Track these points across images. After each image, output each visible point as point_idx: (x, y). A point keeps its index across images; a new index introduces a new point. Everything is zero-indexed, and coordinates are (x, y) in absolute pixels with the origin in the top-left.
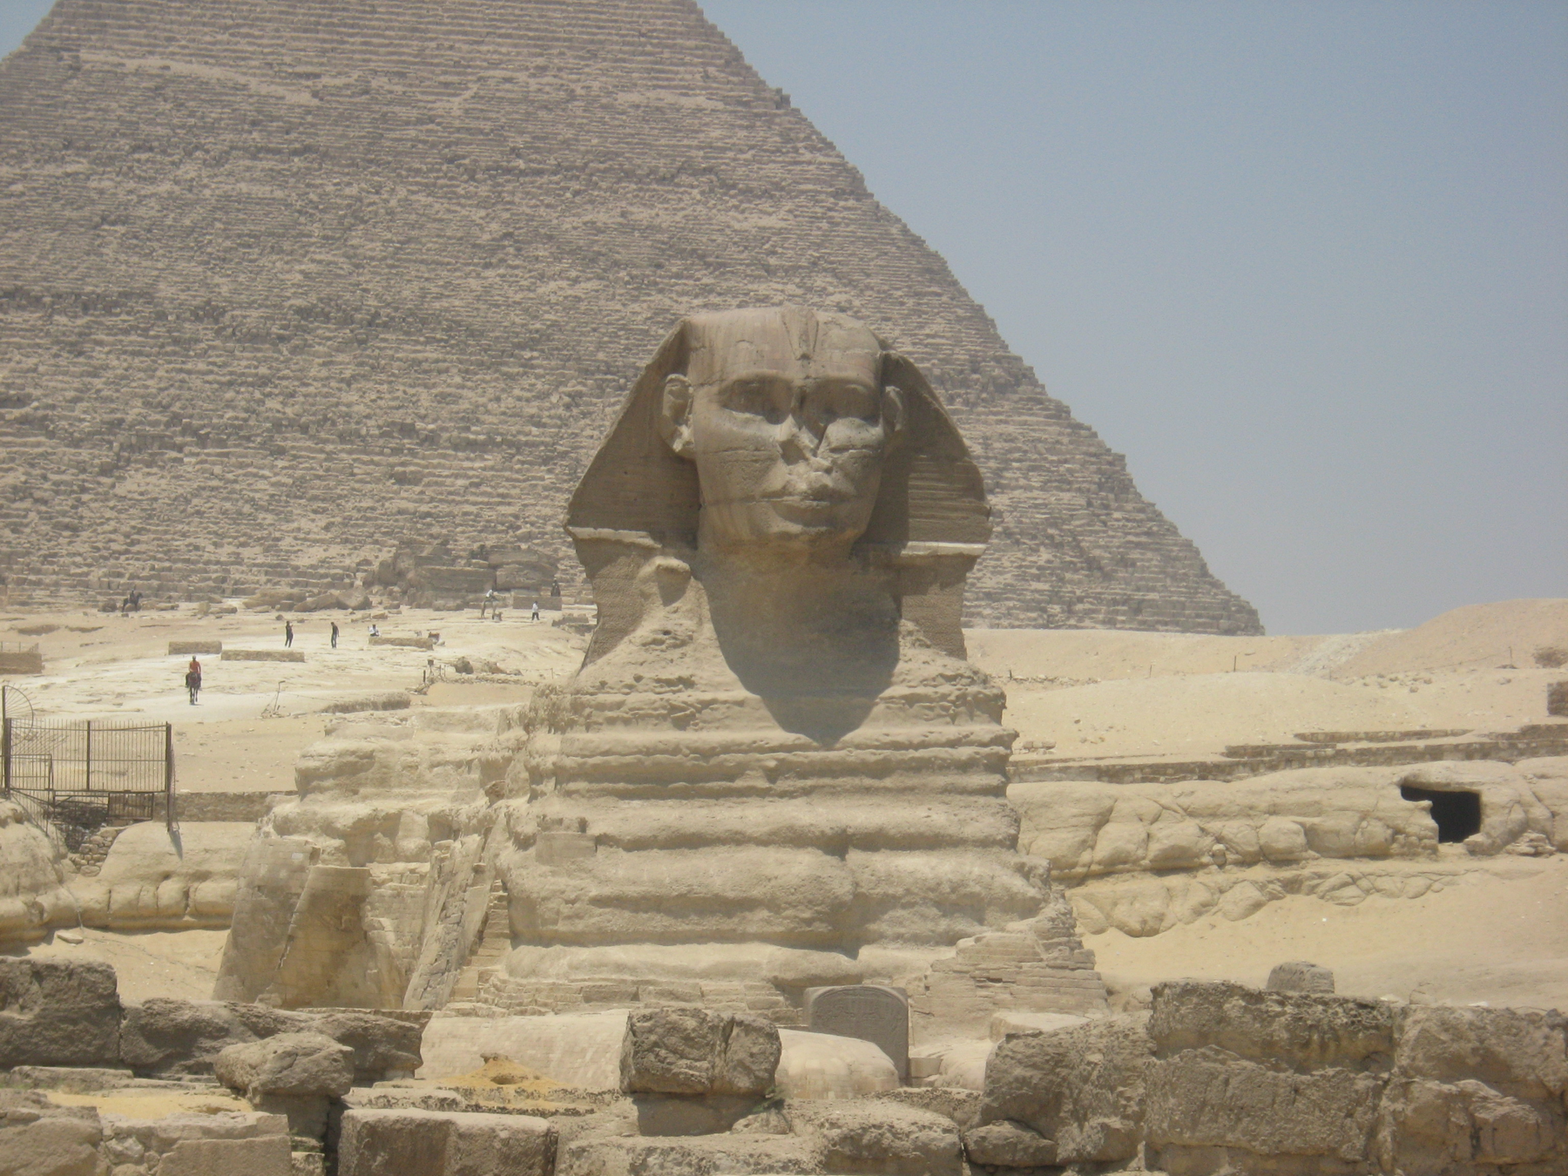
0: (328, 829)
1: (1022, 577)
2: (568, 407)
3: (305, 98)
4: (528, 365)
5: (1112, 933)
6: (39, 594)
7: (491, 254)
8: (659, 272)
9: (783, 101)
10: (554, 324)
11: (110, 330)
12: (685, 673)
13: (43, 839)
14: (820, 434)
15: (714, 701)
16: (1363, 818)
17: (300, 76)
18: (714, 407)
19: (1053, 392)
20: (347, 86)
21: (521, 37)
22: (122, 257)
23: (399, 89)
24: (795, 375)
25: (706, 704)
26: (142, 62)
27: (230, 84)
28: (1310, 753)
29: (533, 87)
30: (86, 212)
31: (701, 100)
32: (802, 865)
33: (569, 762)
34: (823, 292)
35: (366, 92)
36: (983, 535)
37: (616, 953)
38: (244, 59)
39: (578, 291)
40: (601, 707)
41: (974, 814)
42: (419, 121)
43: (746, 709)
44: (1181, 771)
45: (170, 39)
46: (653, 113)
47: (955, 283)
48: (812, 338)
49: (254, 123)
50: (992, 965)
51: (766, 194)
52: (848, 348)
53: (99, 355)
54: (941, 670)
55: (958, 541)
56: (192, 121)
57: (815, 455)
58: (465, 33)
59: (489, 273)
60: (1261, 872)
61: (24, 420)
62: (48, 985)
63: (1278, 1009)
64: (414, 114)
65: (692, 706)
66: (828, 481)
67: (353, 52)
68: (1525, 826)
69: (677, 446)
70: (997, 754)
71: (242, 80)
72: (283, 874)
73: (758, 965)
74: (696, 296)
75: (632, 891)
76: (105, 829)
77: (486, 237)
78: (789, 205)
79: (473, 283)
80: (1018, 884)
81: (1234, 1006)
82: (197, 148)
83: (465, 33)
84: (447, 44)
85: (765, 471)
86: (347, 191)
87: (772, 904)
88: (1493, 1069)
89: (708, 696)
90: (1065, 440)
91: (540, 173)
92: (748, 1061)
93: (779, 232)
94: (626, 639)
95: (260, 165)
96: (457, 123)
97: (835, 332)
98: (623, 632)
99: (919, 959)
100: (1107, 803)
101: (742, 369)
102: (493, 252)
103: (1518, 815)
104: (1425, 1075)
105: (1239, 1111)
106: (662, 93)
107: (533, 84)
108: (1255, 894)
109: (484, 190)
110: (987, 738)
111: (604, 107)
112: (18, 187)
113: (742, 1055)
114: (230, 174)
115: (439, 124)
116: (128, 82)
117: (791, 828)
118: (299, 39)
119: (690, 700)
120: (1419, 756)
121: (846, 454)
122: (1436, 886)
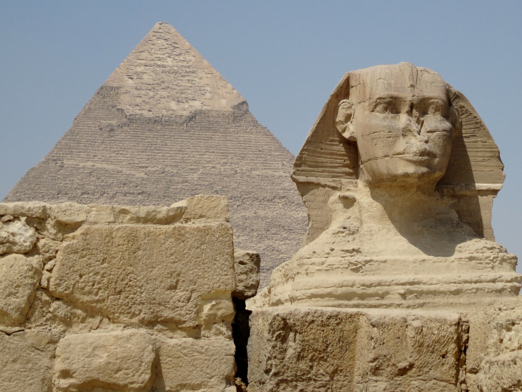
3: (142, 175)
8: (268, 233)
12: (356, 247)
14: (421, 124)
15: (371, 261)
17: (141, 167)
18: (367, 112)
20: (157, 171)
21: (217, 153)
23: (175, 171)
24: (408, 96)
25: (367, 262)
26: (85, 164)
27: (116, 171)
29: (222, 169)
31: (281, 173)
35: (163, 173)
38: (121, 162)
42: (182, 182)
43: (387, 265)
45: (94, 156)
46: (264, 178)
48: (415, 77)
49: (124, 184)
52: (433, 83)
54: (484, 245)
55: (488, 183)
56: (103, 184)
57: (419, 134)
58: (198, 152)
64: (181, 179)
65: (360, 263)
66: (427, 146)
67: (160, 159)
69: (346, 135)
70: (515, 286)
71: (120, 169)
74: (282, 241)
82: (104, 193)
83: (198, 152)
84: (192, 155)
85: (395, 142)
89: (368, 258)
94: (324, 232)
95: (127, 198)
96: (196, 183)
98: (322, 229)
101: (381, 91)
106: (268, 171)
110: (509, 279)
111: (248, 176)
114: (116, 202)
115: (189, 183)
118: (140, 155)
119: (359, 260)
121: (435, 134)
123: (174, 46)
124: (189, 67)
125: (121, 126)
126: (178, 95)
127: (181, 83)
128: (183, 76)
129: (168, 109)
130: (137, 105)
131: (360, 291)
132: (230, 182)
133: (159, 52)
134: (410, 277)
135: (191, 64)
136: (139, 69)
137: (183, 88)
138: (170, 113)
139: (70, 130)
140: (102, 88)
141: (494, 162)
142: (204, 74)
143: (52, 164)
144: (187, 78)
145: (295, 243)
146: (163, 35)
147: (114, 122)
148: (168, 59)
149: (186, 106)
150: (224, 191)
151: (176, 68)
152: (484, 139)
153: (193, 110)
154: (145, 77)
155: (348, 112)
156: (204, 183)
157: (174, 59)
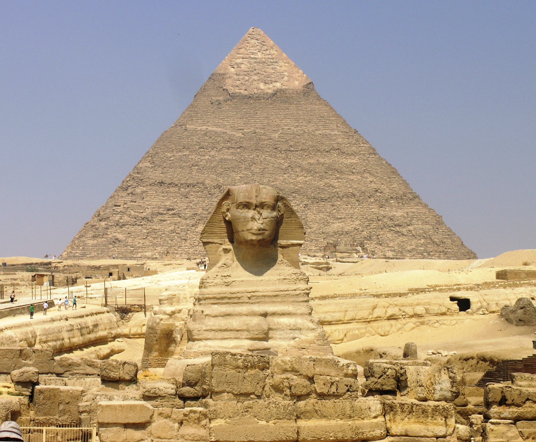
0: (165, 313)
1: (417, 246)
2: (304, 207)
3: (240, 135)
4: (294, 197)
5: (377, 336)
6: (178, 256)
7: (285, 171)
9: (356, 132)
10: (301, 187)
11: (194, 192)
13: (114, 317)
16: (440, 306)
18: (235, 209)
19: (424, 201)
20: (250, 132)
22: (197, 174)
23: (263, 132)
24: (254, 201)
28: (427, 290)
29: (295, 130)
30: (188, 164)
31: (336, 132)
32: (255, 321)
33: (201, 297)
34: (366, 178)
36: (303, 239)
37: (209, 343)
39: (307, 179)
40: (208, 282)
41: (300, 307)
42: (268, 139)
44: (395, 295)
46: (324, 136)
47: (399, 175)
50: (303, 345)
51: (352, 154)
53: (191, 197)
59: (285, 175)
60: (414, 320)
61: (174, 214)
62: (36, 354)
63: (240, 358)
66: (262, 226)
68: (481, 308)
69: (227, 219)
71: (225, 131)
72: (155, 325)
73: (244, 346)
75: (214, 328)
76: (130, 314)
77: (284, 167)
78: (357, 157)
79: (281, 178)
80: (311, 325)
81: (228, 357)
85: (246, 224)
86: (251, 157)
87: (248, 330)
88: (294, 371)
89: (234, 280)
90: (427, 212)
91: (297, 151)
92: (129, 372)
93: (356, 164)
95: (230, 151)
96: (277, 140)
97: (264, 190)
98: (215, 264)
99: (285, 344)
100: (376, 303)
102: (286, 170)
103: (479, 305)
104: (277, 374)
105: (229, 383)
106: (327, 131)
107: (295, 130)
108: (413, 325)
109: (283, 156)
112: (172, 158)
113: (127, 371)
114: (223, 154)
116: (199, 132)
117: (253, 312)
120: (454, 290)
122: (458, 323)
123: (263, 43)
124: (273, 59)
125: (225, 101)
126: (265, 79)
127: (267, 70)
128: (268, 65)
129: (258, 89)
130: (237, 86)
131: (229, 296)
132: (300, 139)
133: (252, 49)
134: (254, 289)
135: (274, 56)
136: (239, 61)
137: (268, 73)
138: (260, 91)
139: (192, 105)
140: (212, 75)
141: (300, 230)
142: (283, 63)
143: (179, 128)
144: (271, 67)
145: (345, 181)
146: (255, 36)
147: (221, 98)
148: (259, 53)
149: (271, 86)
150: (296, 146)
151: (264, 60)
152: (295, 219)
153: (275, 88)
154: (243, 66)
155: (228, 207)
156: (283, 140)
157: (262, 53)
